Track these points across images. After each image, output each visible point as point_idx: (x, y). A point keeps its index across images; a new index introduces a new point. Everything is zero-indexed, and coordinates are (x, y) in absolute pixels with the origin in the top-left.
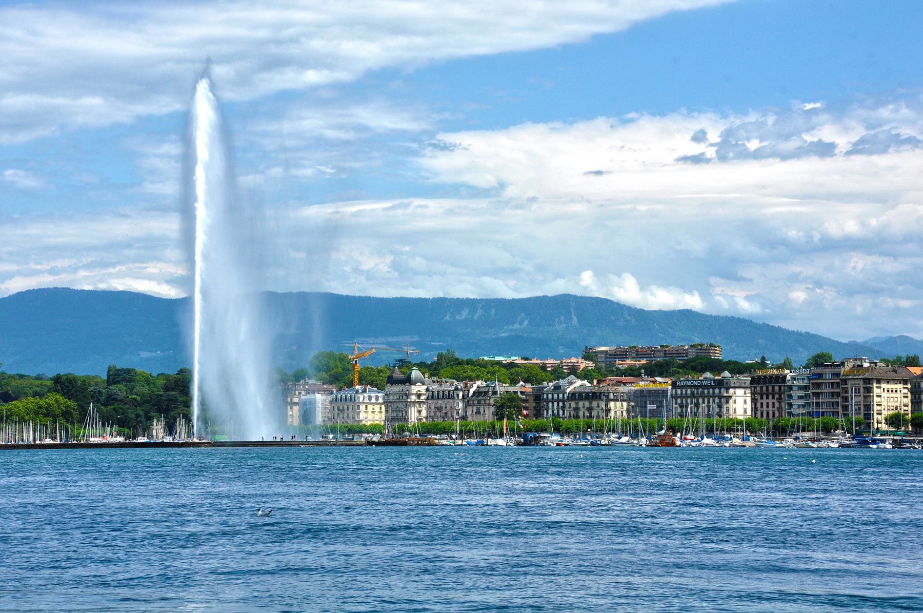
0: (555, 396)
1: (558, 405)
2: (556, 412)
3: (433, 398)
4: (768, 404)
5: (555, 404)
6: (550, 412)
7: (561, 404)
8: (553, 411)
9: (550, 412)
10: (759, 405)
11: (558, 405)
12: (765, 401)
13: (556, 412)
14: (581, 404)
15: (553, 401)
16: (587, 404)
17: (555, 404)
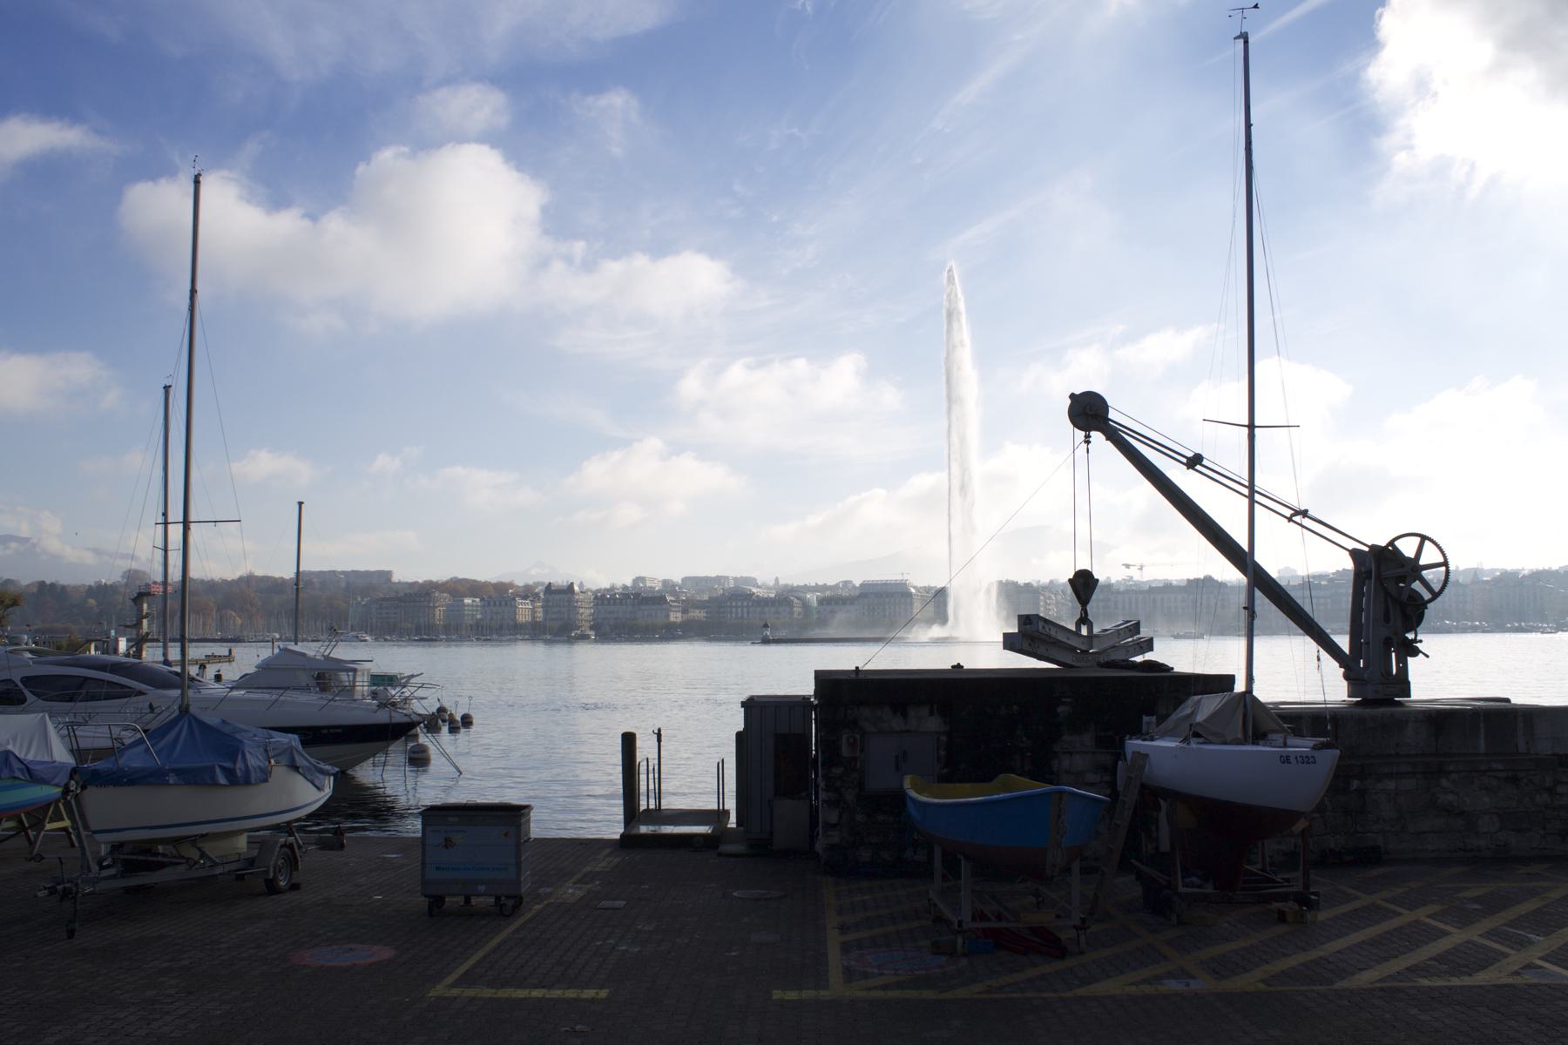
1: (742, 610)
2: (740, 615)
3: (603, 604)
5: (739, 610)
6: (734, 615)
7: (745, 610)
8: (737, 614)
9: (734, 615)
11: (742, 610)
13: (740, 615)
14: (766, 609)
15: (736, 607)
16: (773, 609)
17: (739, 610)
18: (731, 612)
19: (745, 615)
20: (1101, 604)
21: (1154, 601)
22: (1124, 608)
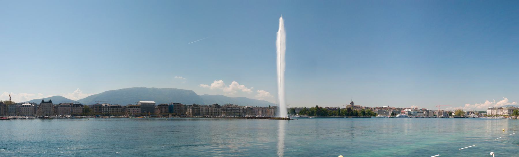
0: (106, 107)
1: (107, 109)
2: (106, 110)
3: (62, 106)
4: (164, 110)
5: (106, 109)
6: (104, 110)
7: (108, 109)
8: (105, 110)
9: (104, 110)
10: (162, 110)
11: (107, 109)
12: (163, 109)
13: (106, 110)
15: (105, 108)
16: (116, 109)
17: (106, 109)
18: (103, 110)
19: (108, 110)
20: (198, 109)
21: (209, 109)
22: (203, 111)
